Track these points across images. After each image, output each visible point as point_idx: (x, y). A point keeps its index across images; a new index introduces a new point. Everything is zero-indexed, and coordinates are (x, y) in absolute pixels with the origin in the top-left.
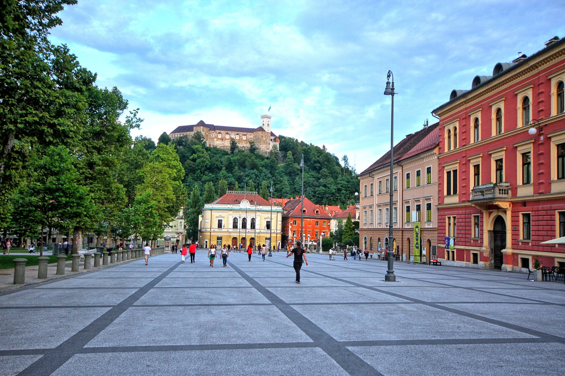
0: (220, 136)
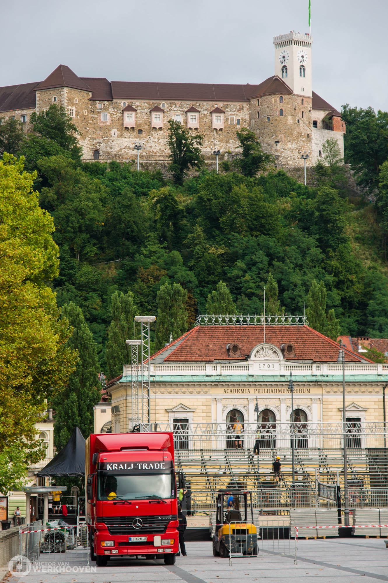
0: (130, 120)
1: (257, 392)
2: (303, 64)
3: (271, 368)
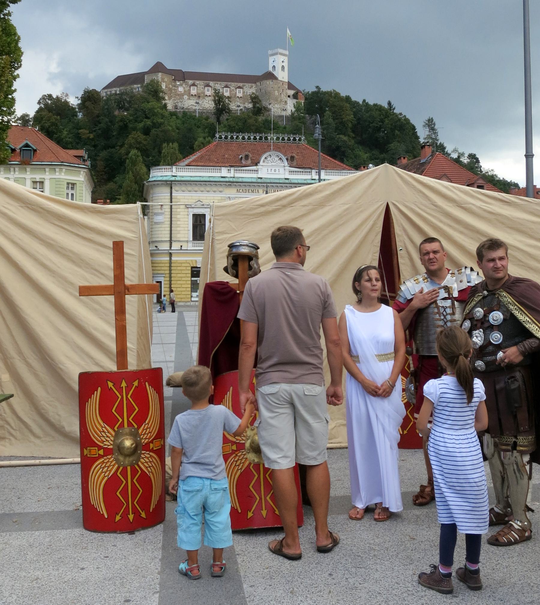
0: (194, 91)
3: (277, 171)
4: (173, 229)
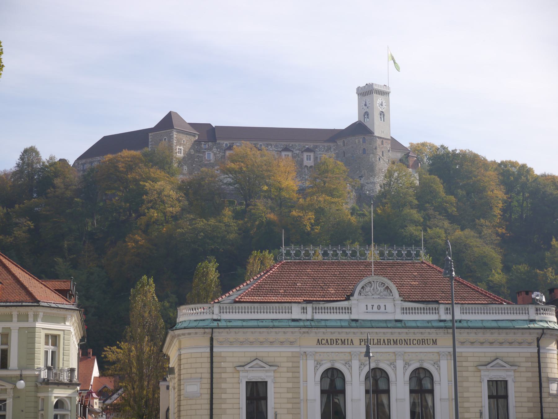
1: (363, 343)
2: (383, 110)
4: (214, 406)
